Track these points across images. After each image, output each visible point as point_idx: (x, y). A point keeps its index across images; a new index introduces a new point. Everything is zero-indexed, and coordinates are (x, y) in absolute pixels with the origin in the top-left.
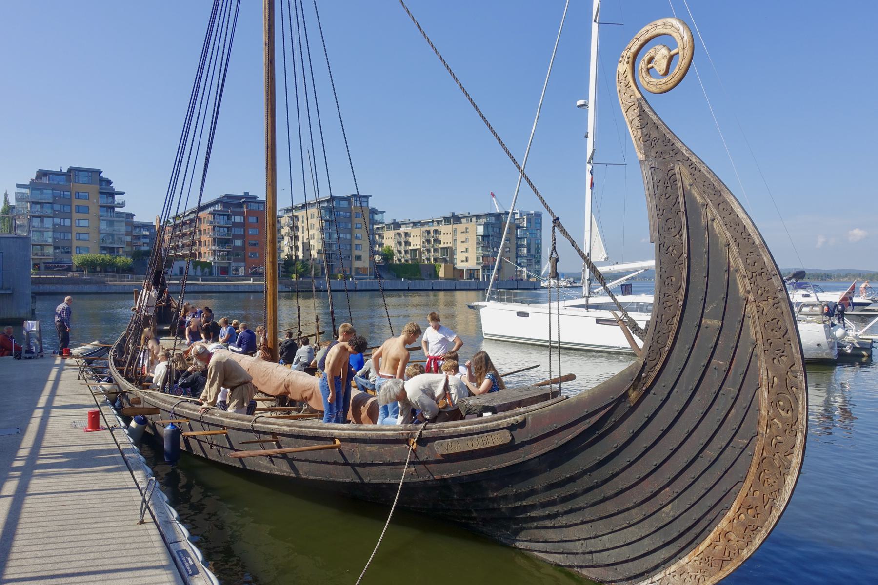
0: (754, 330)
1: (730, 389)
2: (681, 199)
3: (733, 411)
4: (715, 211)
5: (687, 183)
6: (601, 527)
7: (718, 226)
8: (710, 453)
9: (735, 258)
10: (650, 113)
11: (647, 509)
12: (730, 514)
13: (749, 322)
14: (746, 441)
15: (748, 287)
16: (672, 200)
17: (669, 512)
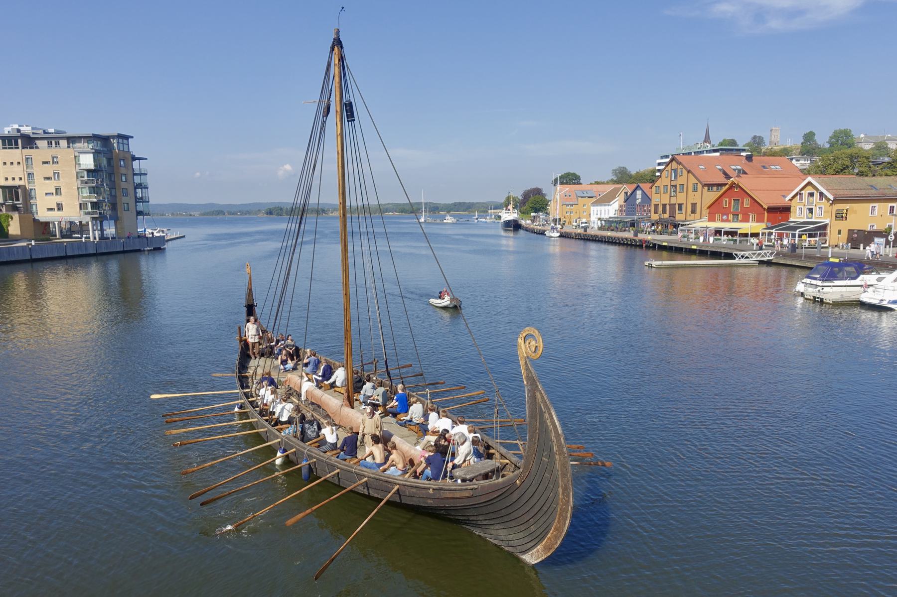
7: (548, 422)
8: (545, 508)
9: (553, 435)
11: (526, 526)
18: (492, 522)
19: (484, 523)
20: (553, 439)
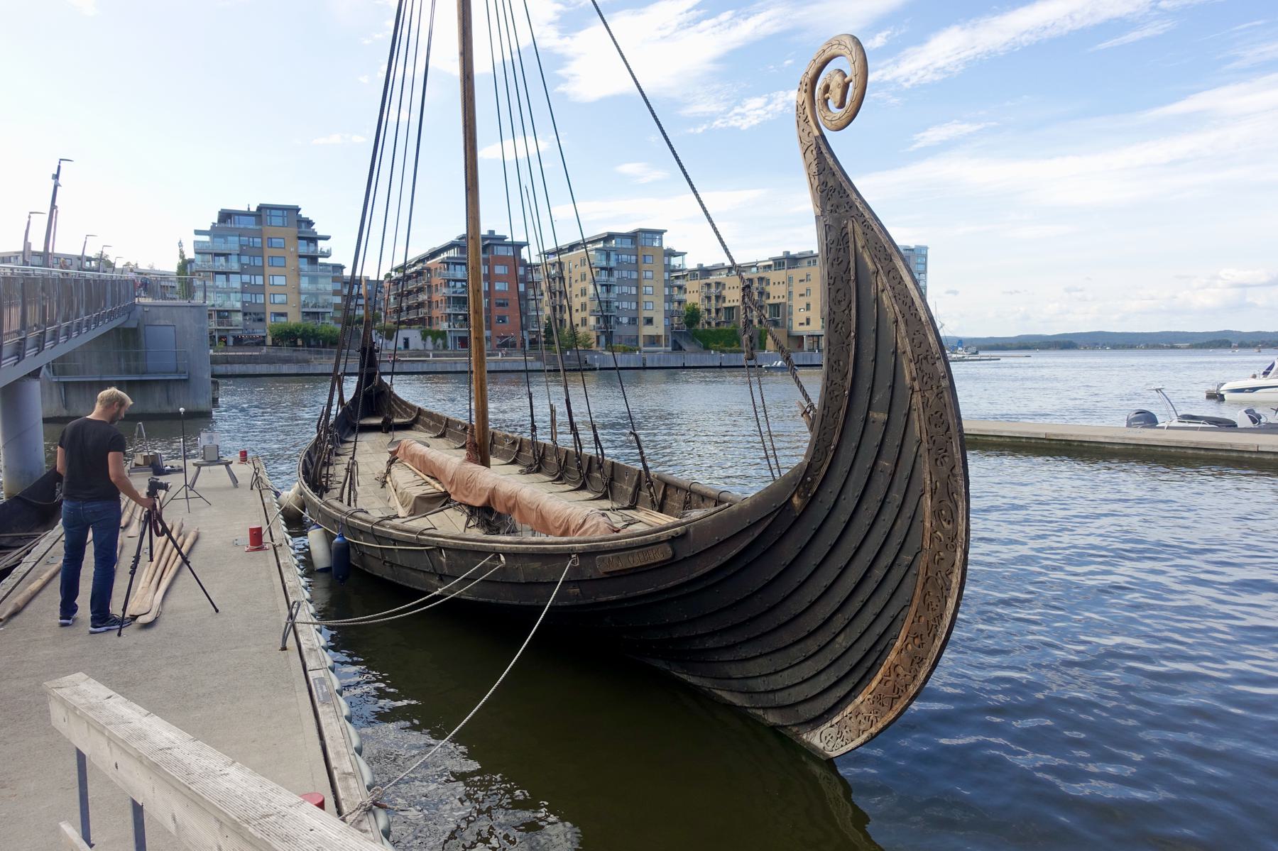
0: (918, 425)
1: (896, 496)
2: (852, 265)
3: (899, 522)
4: (885, 280)
5: (859, 245)
6: (780, 660)
8: (878, 573)
10: (827, 156)
11: (822, 638)
12: (898, 644)
13: (915, 415)
14: (911, 558)
15: (914, 374)
16: (845, 264)
17: (842, 642)
18: (731, 639)
19: (710, 644)
20: (905, 344)
